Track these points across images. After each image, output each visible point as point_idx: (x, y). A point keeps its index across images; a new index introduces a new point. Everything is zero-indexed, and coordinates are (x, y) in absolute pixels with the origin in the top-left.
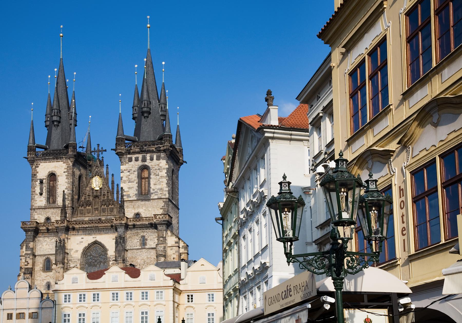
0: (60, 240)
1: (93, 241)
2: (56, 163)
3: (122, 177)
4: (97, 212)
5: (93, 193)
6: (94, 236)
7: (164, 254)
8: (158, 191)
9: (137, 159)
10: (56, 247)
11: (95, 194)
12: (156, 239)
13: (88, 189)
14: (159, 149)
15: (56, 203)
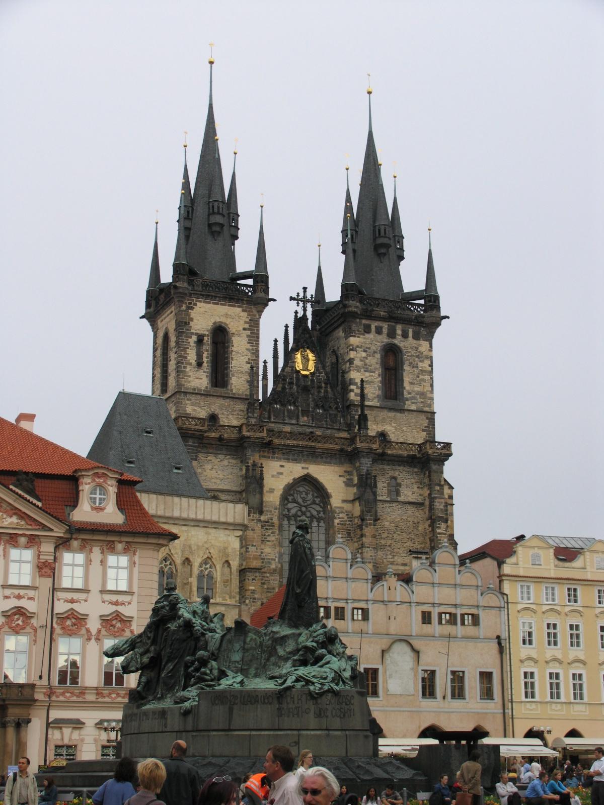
0: (254, 465)
1: (302, 474)
2: (227, 307)
3: (353, 359)
4: (306, 418)
5: (298, 379)
6: (303, 465)
7: (445, 517)
8: (418, 397)
9: (379, 331)
10: (246, 477)
11: (302, 383)
12: (415, 486)
13: (288, 369)
14: (420, 320)
15: (229, 387)
